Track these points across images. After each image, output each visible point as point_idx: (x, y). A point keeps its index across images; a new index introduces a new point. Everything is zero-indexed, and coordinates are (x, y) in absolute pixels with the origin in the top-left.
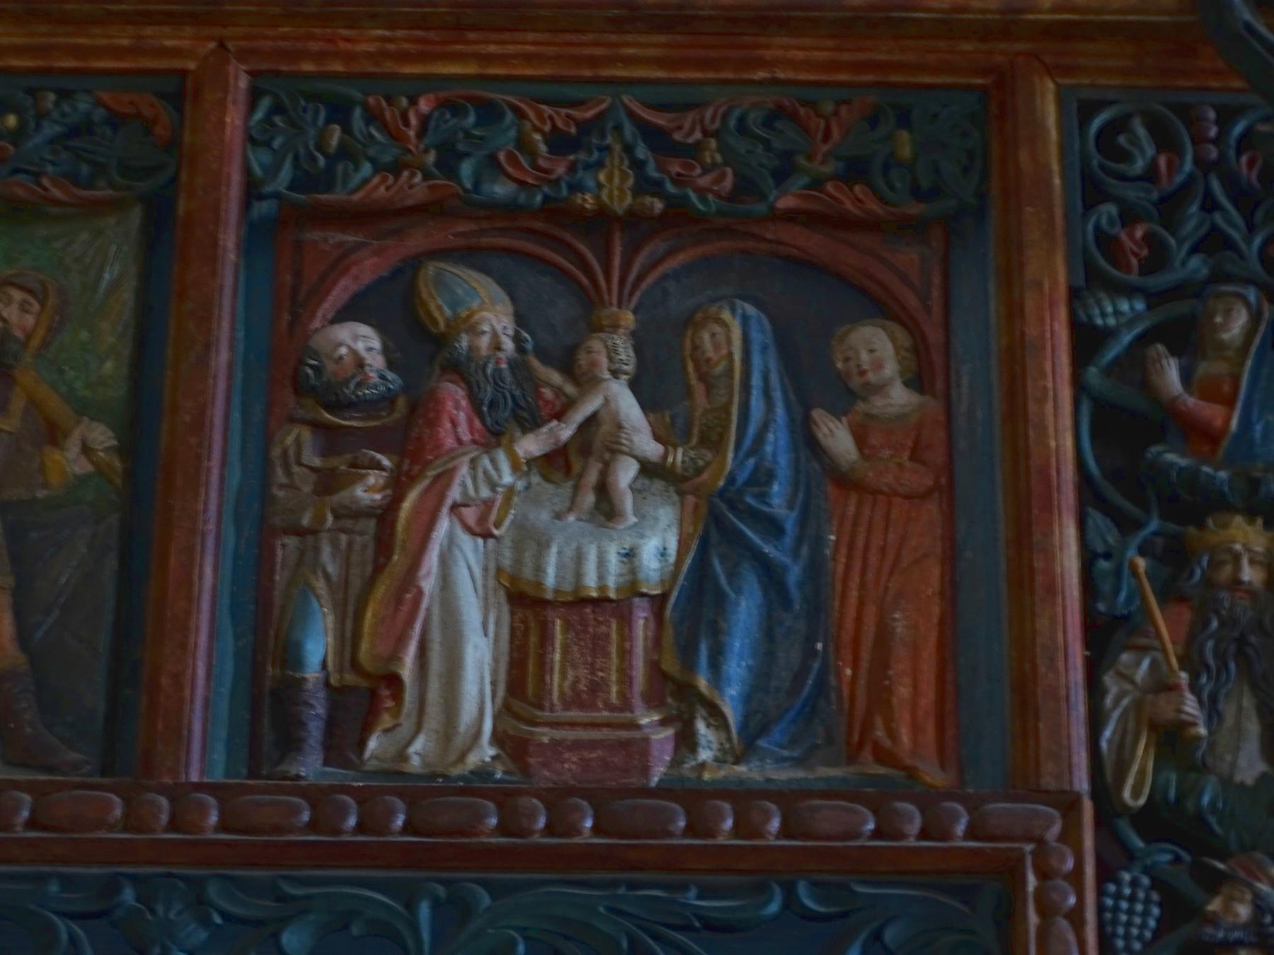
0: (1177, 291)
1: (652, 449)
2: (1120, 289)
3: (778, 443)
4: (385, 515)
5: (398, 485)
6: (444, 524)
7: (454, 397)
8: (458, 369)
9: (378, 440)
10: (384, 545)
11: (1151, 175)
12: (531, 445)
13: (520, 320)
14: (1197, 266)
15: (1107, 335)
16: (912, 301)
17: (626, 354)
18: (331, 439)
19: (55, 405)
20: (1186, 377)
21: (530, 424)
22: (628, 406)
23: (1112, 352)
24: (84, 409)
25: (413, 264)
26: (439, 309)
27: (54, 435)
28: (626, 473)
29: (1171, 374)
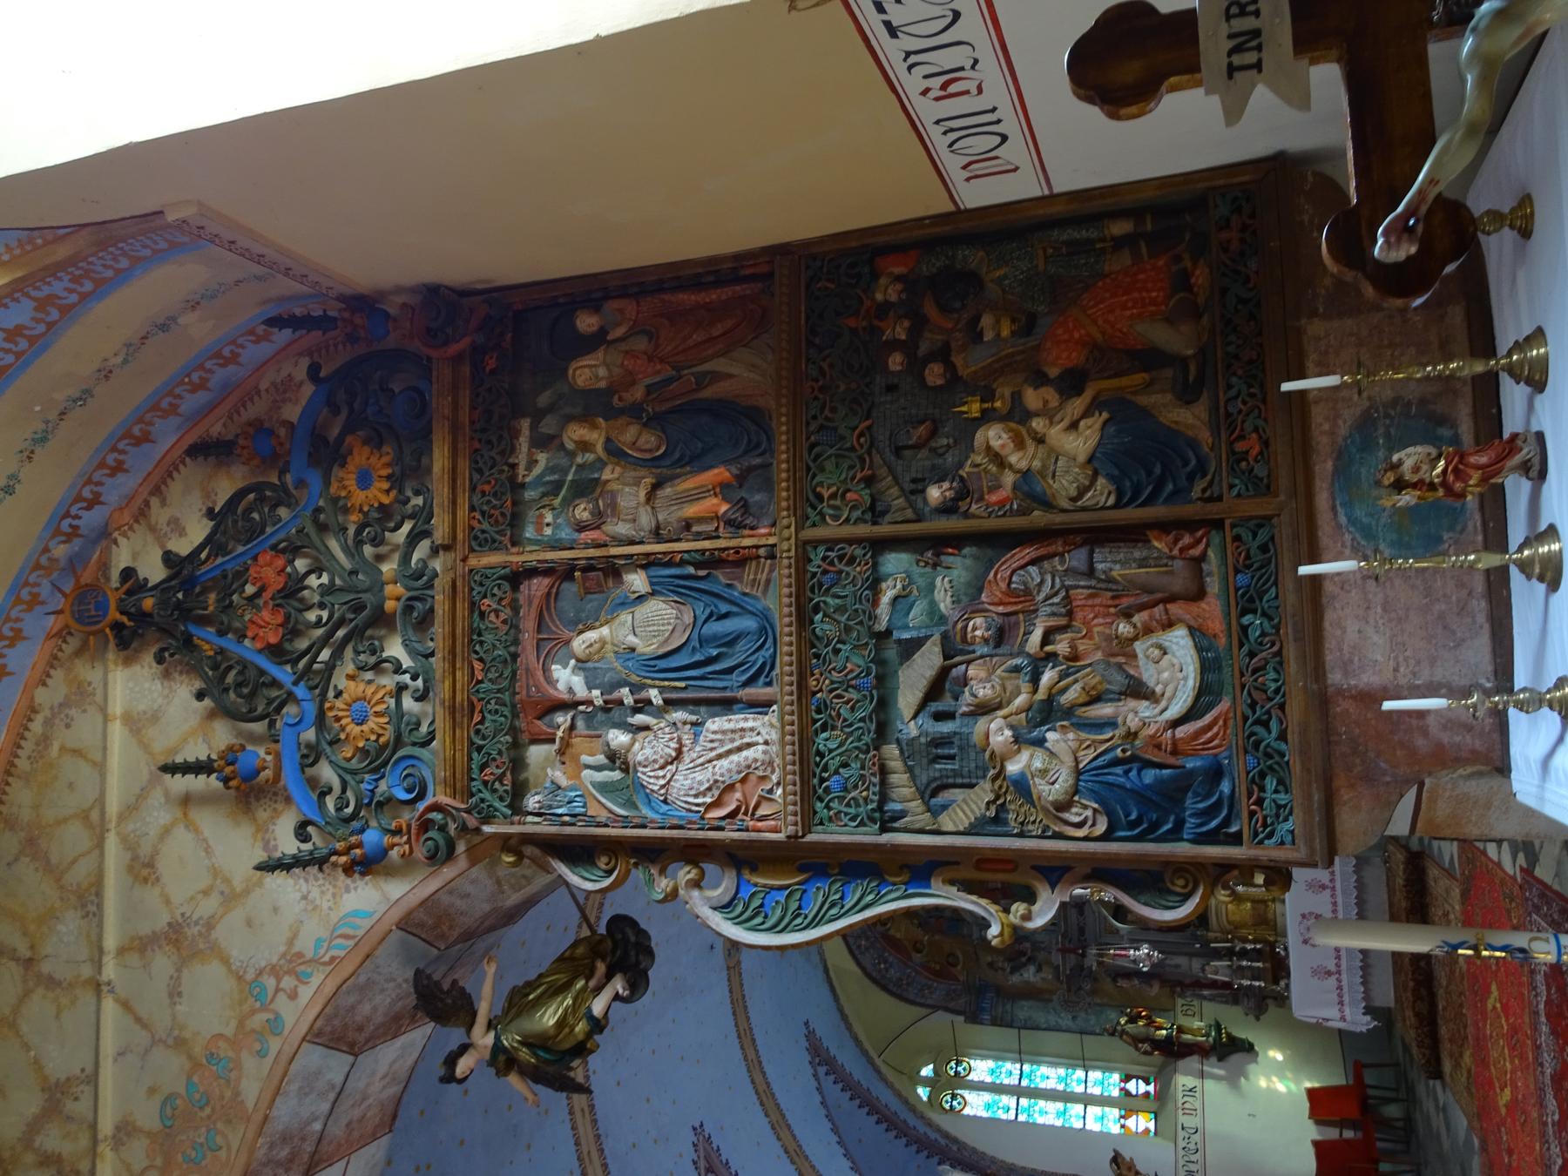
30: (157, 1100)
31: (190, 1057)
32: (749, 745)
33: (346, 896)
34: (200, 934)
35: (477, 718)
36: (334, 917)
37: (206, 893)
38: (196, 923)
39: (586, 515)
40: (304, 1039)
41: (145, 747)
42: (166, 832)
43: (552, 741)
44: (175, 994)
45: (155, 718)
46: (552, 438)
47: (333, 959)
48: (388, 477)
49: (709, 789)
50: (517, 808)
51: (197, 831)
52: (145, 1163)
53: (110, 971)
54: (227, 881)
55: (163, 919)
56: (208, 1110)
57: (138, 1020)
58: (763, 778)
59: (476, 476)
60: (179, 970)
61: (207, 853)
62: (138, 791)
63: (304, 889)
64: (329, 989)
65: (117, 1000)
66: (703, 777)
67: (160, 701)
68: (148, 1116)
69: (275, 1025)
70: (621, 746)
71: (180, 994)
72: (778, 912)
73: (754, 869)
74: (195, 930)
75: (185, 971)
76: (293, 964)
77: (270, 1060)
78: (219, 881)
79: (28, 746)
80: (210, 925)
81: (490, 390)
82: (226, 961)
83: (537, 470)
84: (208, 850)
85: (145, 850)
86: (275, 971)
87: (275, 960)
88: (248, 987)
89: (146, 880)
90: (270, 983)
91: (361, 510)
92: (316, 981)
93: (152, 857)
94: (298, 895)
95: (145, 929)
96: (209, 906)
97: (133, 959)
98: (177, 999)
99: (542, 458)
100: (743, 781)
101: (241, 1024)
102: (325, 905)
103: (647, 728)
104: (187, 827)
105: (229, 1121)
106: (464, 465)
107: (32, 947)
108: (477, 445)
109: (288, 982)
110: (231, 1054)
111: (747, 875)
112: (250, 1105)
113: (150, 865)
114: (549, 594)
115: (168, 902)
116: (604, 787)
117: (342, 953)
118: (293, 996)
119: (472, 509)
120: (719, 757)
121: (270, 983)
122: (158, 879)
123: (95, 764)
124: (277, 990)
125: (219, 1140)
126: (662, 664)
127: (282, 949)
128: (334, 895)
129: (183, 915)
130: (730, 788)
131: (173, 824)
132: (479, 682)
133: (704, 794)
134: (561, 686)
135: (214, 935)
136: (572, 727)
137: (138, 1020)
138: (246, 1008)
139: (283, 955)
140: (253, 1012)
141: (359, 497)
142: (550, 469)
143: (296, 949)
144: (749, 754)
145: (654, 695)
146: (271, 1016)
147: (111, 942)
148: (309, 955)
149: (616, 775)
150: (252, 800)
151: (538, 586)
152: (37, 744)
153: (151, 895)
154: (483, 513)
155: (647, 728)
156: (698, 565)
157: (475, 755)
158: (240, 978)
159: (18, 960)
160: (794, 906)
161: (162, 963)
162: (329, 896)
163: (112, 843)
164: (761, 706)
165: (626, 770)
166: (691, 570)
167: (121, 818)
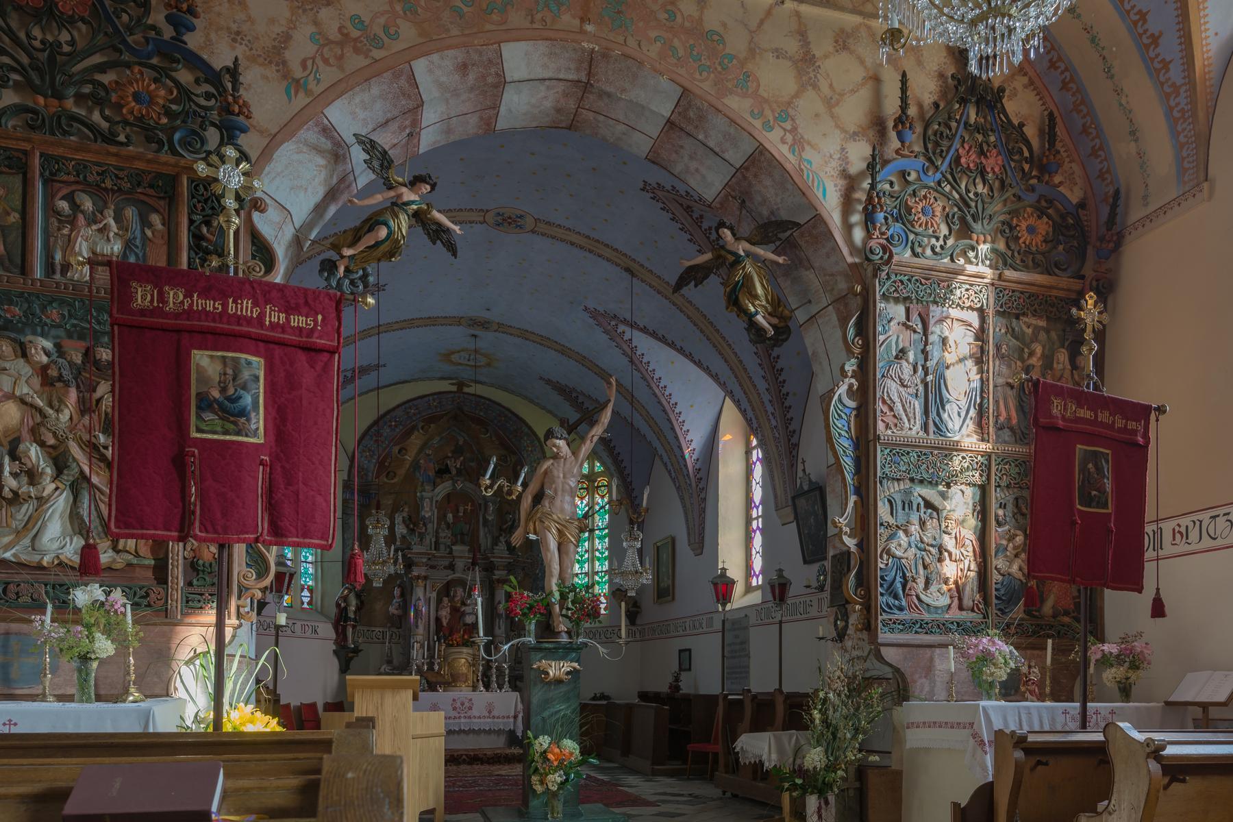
0: (207, 216)
1: (116, 231)
2: (197, 214)
3: (138, 234)
4: (70, 236)
5: (72, 231)
6: (80, 239)
7: (81, 217)
8: (82, 212)
9: (68, 222)
10: (69, 241)
11: (203, 195)
12: (94, 227)
13: (94, 204)
14: (210, 212)
15: (195, 221)
16: (162, 210)
17: (112, 214)
18: (60, 221)
19: (8, 208)
20: (208, 231)
21: (95, 223)
22: (112, 222)
23: (195, 224)
24: (13, 210)
25: (73, 192)
26: (78, 201)
27: (8, 214)
28: (111, 234)
29: (204, 230)
32: (909, 420)
33: (832, 184)
34: (810, 78)
35: (923, 281)
36: (822, 174)
37: (831, 86)
38: (815, 77)
39: (1003, 351)
40: (761, 144)
42: (862, 62)
44: (779, 53)
46: (1036, 337)
47: (802, 170)
48: (1031, 243)
49: (891, 399)
50: (885, 297)
51: (863, 85)
54: (837, 104)
55: (818, 54)
56: (719, 69)
57: (762, 22)
58: (896, 425)
59: (1027, 295)
60: (790, 58)
61: (852, 90)
63: (835, 157)
64: (788, 167)
66: (896, 398)
67: (928, 68)
69: (768, 127)
70: (908, 357)
71: (778, 57)
72: (840, 426)
73: (856, 416)
75: (790, 64)
76: (798, 144)
77: (747, 116)
78: (837, 96)
80: (815, 87)
81: (1063, 307)
82: (797, 95)
83: (1025, 328)
84: (853, 91)
86: (794, 130)
87: (800, 130)
88: (784, 112)
89: (836, 42)
90: (788, 126)
91: (1017, 225)
92: (790, 157)
93: (848, 49)
94: (832, 152)
95: (811, 36)
96: (825, 89)
98: (775, 54)
99: (1030, 331)
100: (894, 416)
101: (766, 101)
102: (828, 169)
103: (915, 371)
104: (864, 78)
106: (1034, 290)
108: (1041, 297)
109: (789, 138)
110: (750, 91)
111: (854, 413)
112: (726, 101)
113: (845, 47)
114: (971, 326)
115: (826, 57)
116: (889, 346)
117: (805, 177)
118: (783, 141)
119: (1013, 291)
120: (903, 406)
121: (788, 126)
122: (837, 51)
124: (785, 130)
125: (704, 74)
126: (942, 381)
127: (806, 137)
128: (832, 176)
129: (819, 67)
130: (891, 409)
131: (865, 67)
132: (939, 284)
133: (889, 396)
134: (934, 329)
135: (810, 88)
137: (762, 22)
139: (802, 137)
140: (773, 111)
141: (1024, 225)
142: (1023, 333)
143: (807, 148)
144: (906, 421)
145: (930, 378)
146: (771, 123)
148: (804, 156)
149: (894, 354)
153: (827, 45)
154: (1011, 297)
155: (915, 371)
156: (981, 405)
157: (906, 278)
158: (789, 103)
160: (843, 433)
161: (792, 46)
162: (832, 173)
163: (855, 19)
164: (925, 427)
165: (896, 357)
167: (869, 28)
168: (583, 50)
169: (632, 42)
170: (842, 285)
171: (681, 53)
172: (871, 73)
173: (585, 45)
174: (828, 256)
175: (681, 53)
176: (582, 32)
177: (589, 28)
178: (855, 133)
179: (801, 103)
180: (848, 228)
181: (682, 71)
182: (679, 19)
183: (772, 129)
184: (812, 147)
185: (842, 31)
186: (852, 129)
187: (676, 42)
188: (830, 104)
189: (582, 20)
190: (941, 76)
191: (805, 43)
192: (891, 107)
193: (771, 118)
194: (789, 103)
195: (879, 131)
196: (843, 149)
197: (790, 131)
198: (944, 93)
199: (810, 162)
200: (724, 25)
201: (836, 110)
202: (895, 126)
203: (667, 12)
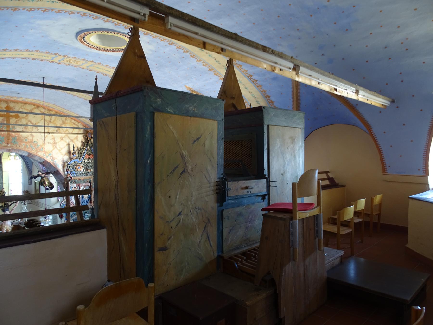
30: (37, 141)
31: (42, 145)
33: (61, 165)
37: (60, 147)
41: (74, 139)
43: (76, 187)
44: (49, 143)
45: (77, 140)
51: (66, 146)
52: (29, 139)
53: (51, 134)
54: (61, 150)
56: (37, 148)
60: (51, 144)
62: (70, 138)
64: (51, 163)
65: (47, 135)
68: (35, 139)
74: (56, 146)
79: (74, 122)
80: (56, 148)
82: (53, 150)
84: (64, 147)
85: (64, 139)
89: (61, 139)
90: (51, 156)
93: (63, 140)
95: (55, 139)
96: (58, 147)
97: (52, 137)
105: (36, 151)
107: (52, 122)
109: (51, 158)
112: (38, 154)
113: (62, 140)
115: (59, 142)
118: (50, 159)
123: (73, 132)
124: (51, 157)
125: (34, 149)
135: (55, 148)
136: (77, 189)
138: (48, 153)
140: (48, 154)
143: (55, 159)
146: (48, 156)
147: (54, 135)
150: (69, 153)
151: (89, 184)
152: (75, 123)
153: (59, 140)
158: (51, 152)
159: (50, 120)
161: (52, 141)
163: (65, 135)
166: (90, 199)
167: (67, 136)
168: (8, 149)
169: (18, 146)
170: (63, 181)
171: (28, 146)
172: (68, 144)
173: (8, 148)
174: (60, 176)
175: (28, 146)
176: (7, 146)
177: (9, 145)
178: (65, 155)
179: (54, 151)
180: (64, 171)
181: (29, 150)
182: (28, 140)
183: (48, 157)
184: (56, 159)
185: (62, 137)
186: (64, 154)
187: (28, 145)
188: (59, 151)
189: (7, 144)
190: (82, 142)
191: (54, 140)
192: (72, 149)
193: (48, 155)
194: (51, 152)
195: (70, 154)
196: (62, 158)
197: (52, 157)
198: (82, 145)
199: (56, 162)
200: (38, 140)
201: (61, 151)
202: (72, 154)
203: (25, 139)
